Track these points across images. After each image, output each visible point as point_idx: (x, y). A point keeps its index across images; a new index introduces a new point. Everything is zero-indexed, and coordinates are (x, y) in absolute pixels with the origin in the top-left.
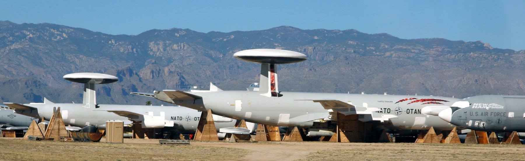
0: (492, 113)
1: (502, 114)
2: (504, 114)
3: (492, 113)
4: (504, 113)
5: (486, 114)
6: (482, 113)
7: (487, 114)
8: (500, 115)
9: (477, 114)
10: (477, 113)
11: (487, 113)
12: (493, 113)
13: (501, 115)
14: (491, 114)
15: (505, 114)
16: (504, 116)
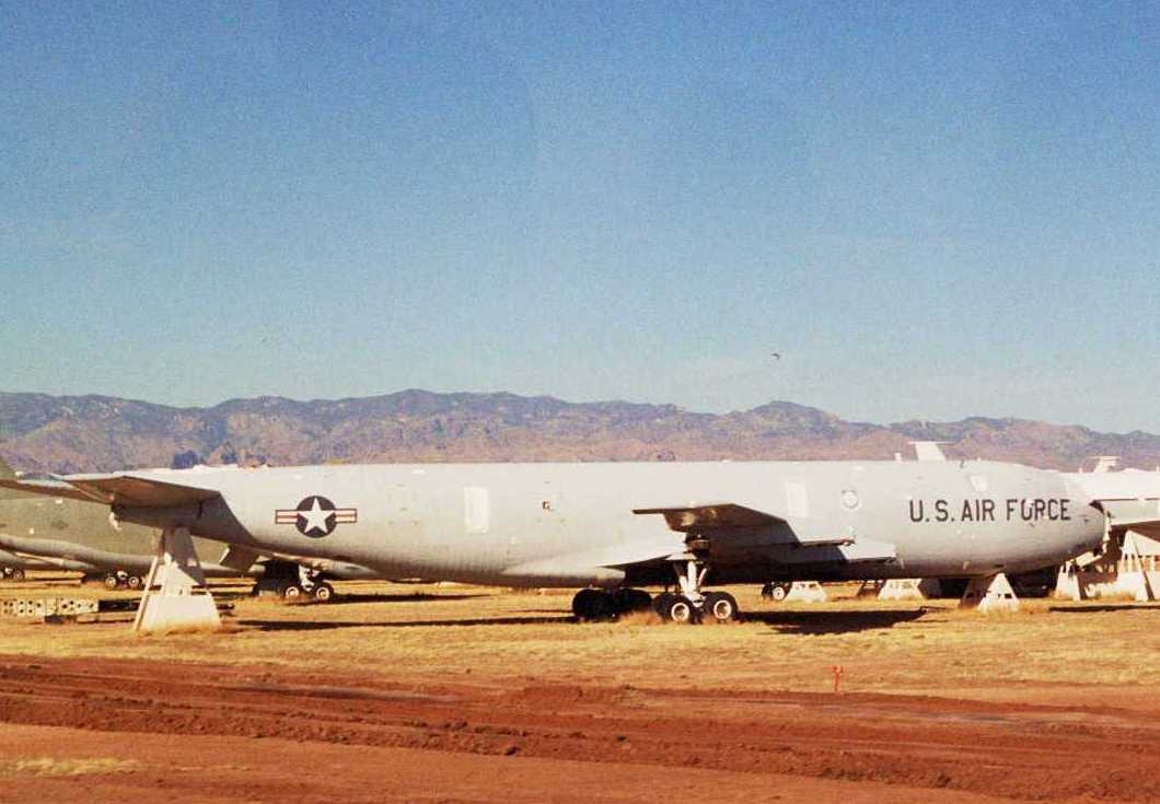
0: (1012, 505)
1: (1053, 504)
2: (1063, 510)
3: (1012, 505)
4: (1063, 501)
5: (985, 510)
6: (967, 505)
7: (990, 510)
8: (1046, 511)
9: (940, 510)
10: (941, 506)
11: (988, 506)
12: (1016, 501)
13: (1053, 515)
14: (1010, 510)
15: (1065, 505)
16: (1063, 518)
